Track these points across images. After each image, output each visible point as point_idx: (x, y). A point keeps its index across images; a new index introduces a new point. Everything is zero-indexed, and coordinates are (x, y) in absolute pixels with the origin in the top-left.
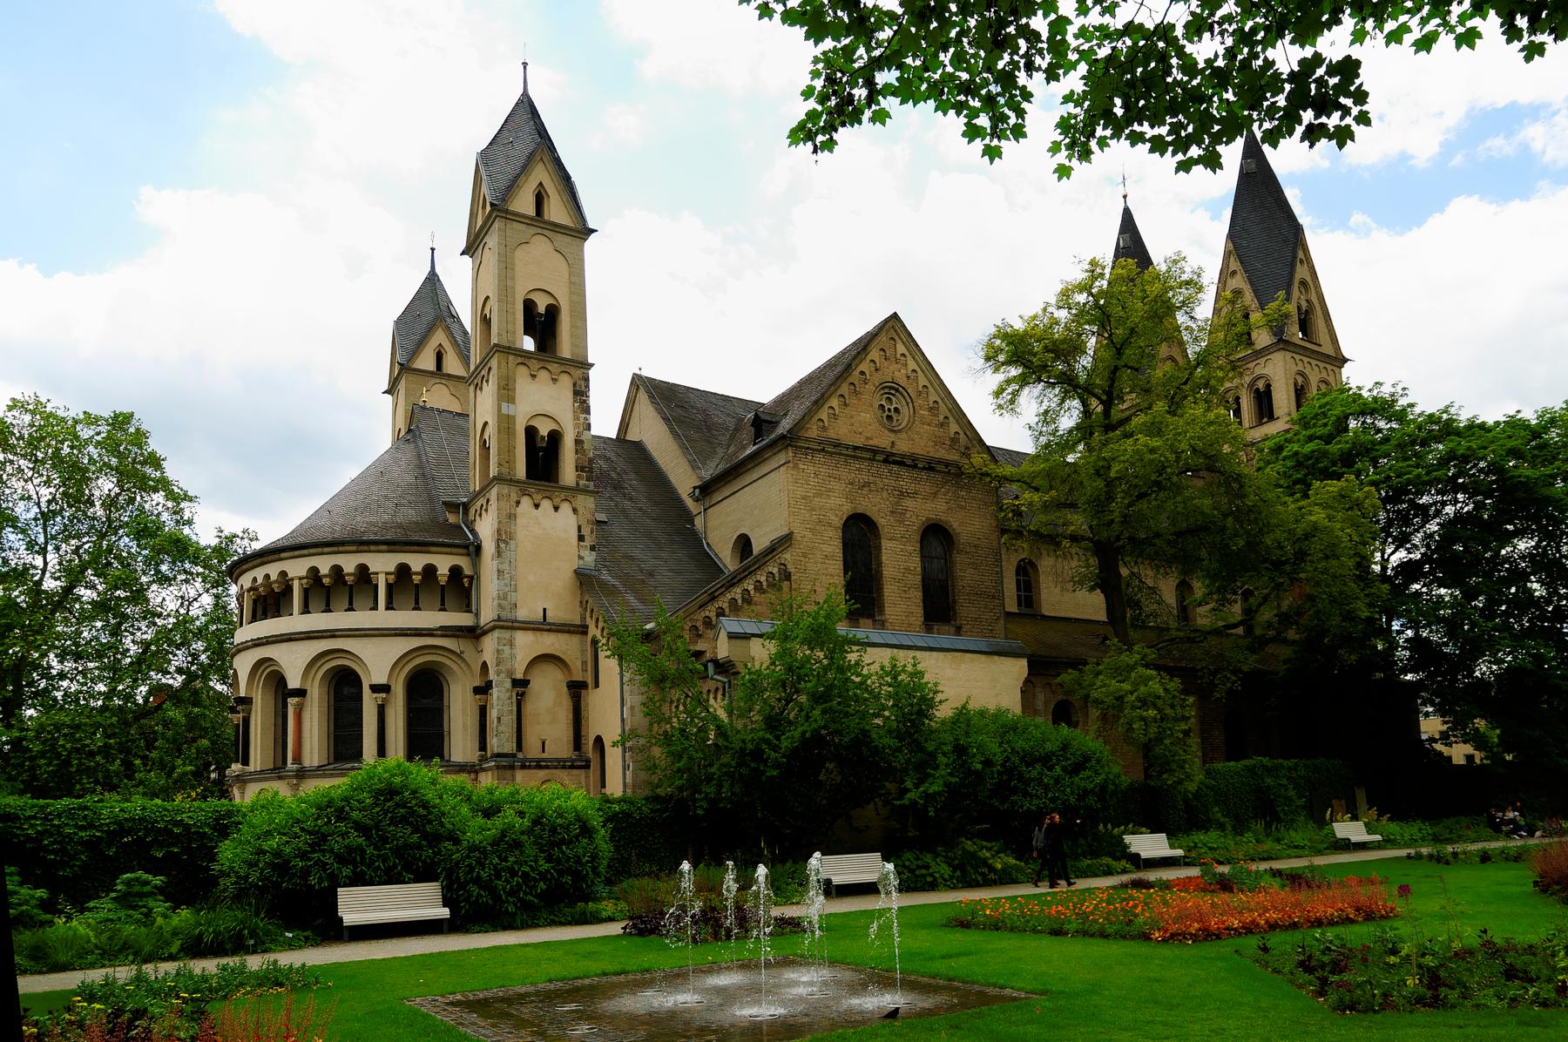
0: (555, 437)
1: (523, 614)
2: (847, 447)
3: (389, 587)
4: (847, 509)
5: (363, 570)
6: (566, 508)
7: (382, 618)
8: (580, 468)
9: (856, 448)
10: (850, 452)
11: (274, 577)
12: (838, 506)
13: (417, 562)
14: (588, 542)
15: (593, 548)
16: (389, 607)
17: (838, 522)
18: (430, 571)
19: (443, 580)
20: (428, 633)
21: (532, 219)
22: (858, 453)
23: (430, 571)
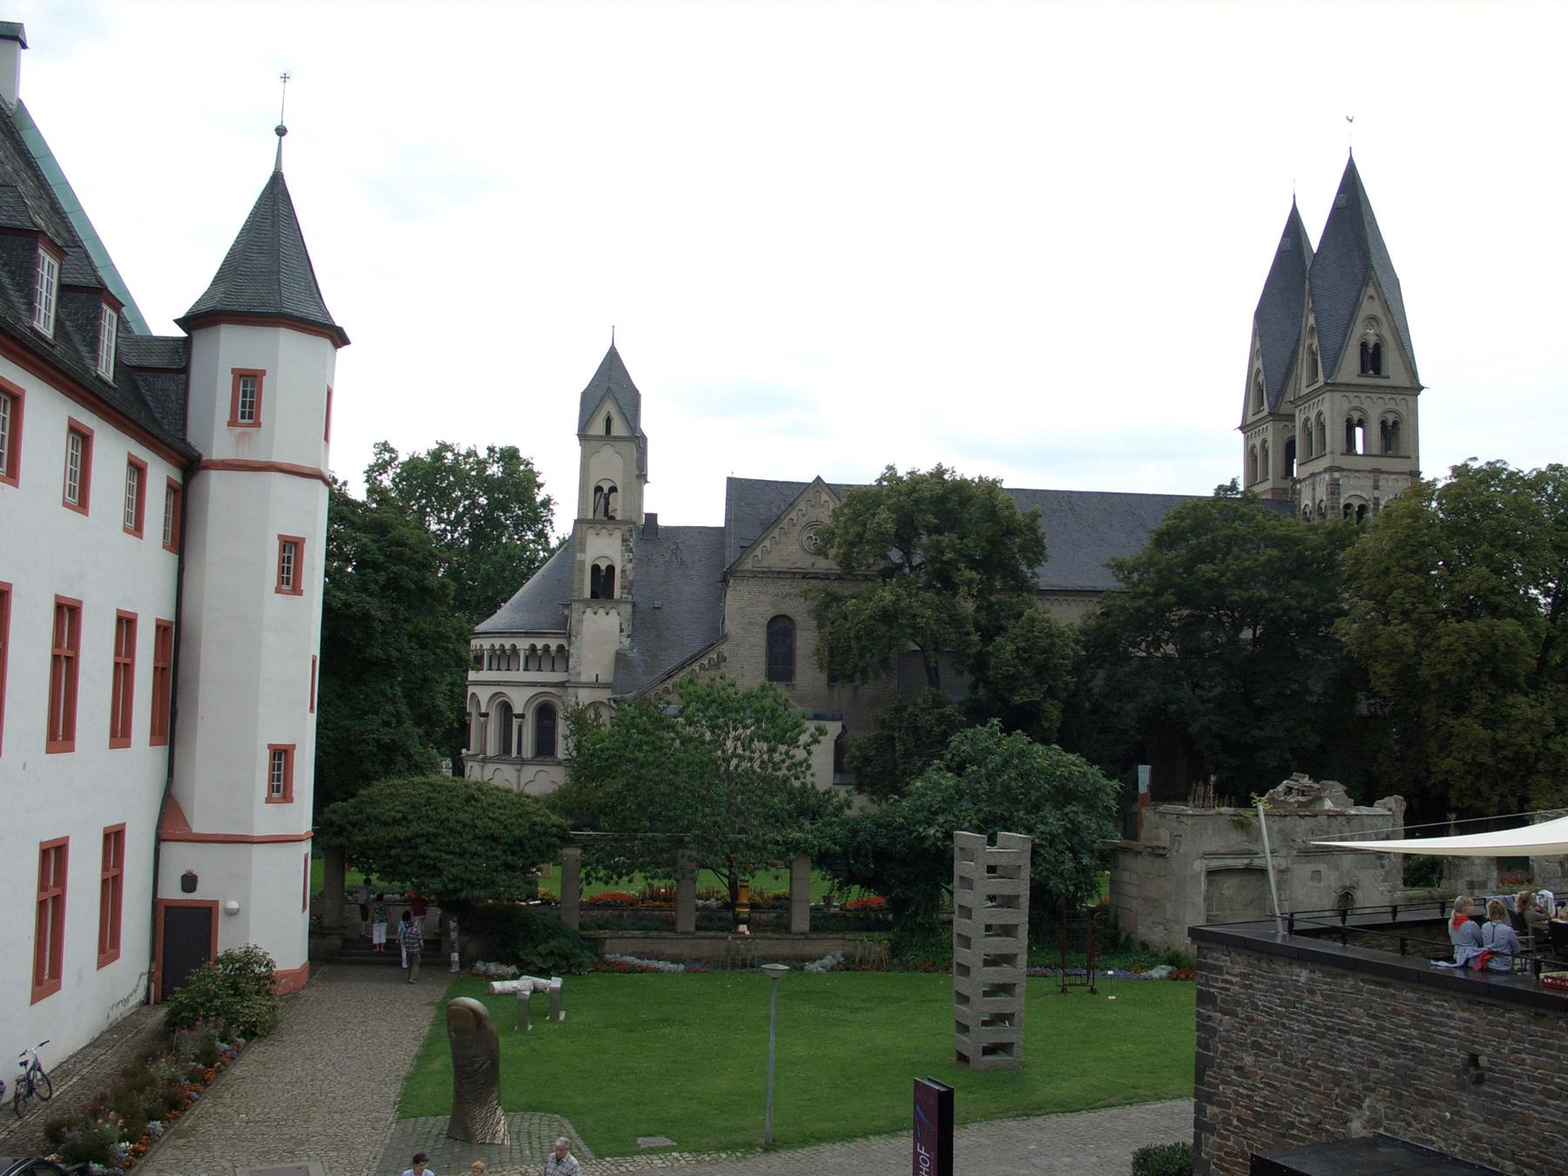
0: (611, 569)
1: (583, 679)
2: (773, 572)
3: (527, 658)
4: (772, 613)
5: (514, 646)
6: (613, 613)
7: (519, 675)
8: (623, 587)
9: (779, 573)
10: (775, 575)
11: (497, 647)
12: (766, 611)
13: (540, 643)
14: (625, 633)
15: (628, 636)
16: (526, 669)
17: (764, 622)
18: (547, 647)
19: (553, 654)
20: (544, 685)
21: (601, 437)
22: (781, 575)
23: (547, 647)
